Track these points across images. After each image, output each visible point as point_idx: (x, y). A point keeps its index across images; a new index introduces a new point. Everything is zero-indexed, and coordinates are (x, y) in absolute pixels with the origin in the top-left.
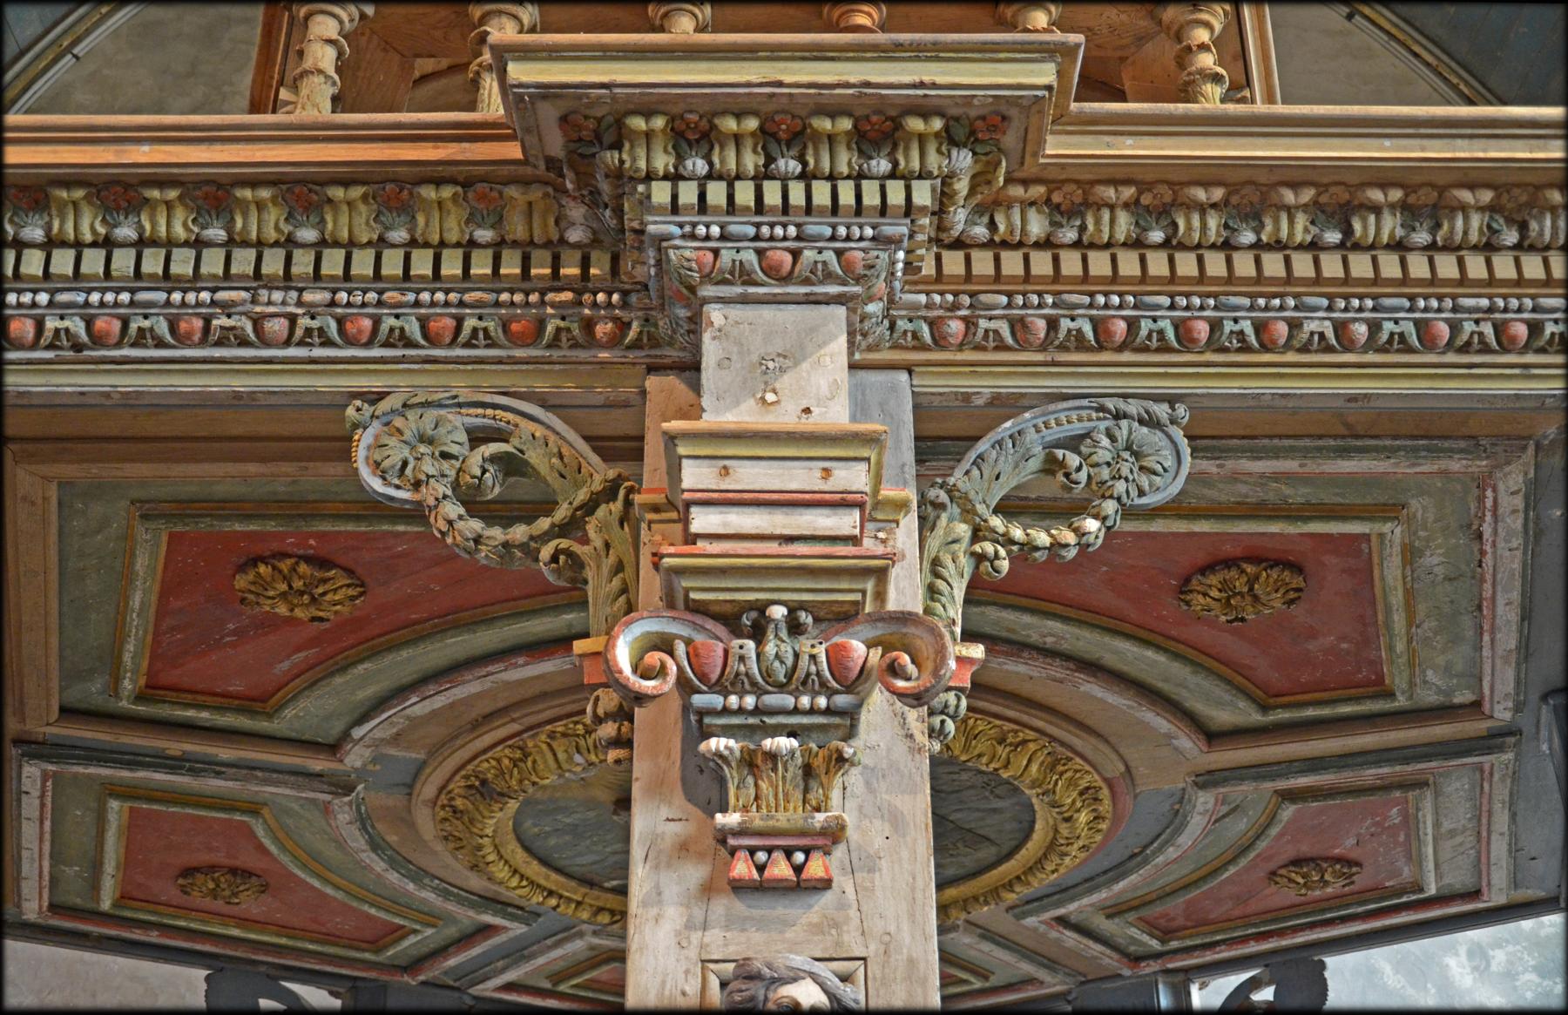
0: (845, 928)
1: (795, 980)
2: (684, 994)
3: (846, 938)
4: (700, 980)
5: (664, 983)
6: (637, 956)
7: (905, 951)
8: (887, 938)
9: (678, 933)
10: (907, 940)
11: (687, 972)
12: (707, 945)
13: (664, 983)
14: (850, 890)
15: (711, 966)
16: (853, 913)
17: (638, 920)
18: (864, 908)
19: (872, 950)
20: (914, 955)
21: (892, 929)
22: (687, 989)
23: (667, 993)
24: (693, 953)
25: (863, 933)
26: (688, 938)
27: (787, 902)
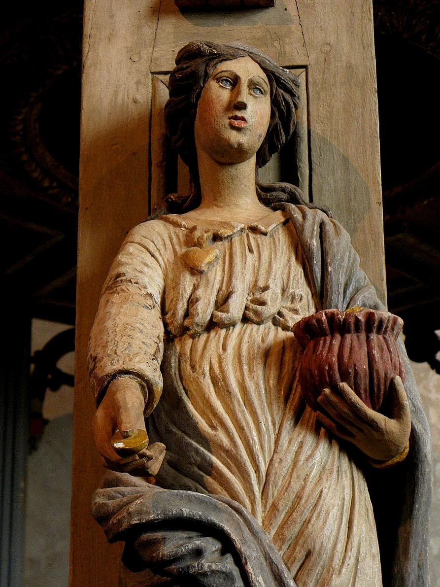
0: (287, 40)
1: (234, 57)
2: (135, 101)
3: (287, 49)
4: (150, 89)
5: (116, 93)
6: (91, 71)
7: (344, 58)
8: (328, 48)
9: (129, 50)
10: (346, 49)
11: (138, 83)
12: (157, 59)
13: (116, 93)
14: (292, 8)
15: (161, 77)
16: (294, 27)
17: (92, 40)
18: (305, 22)
19: (312, 59)
20: (353, 62)
21: (332, 39)
22: (139, 97)
23: (119, 101)
24: (144, 66)
25: (304, 45)
26: (139, 53)
27: (232, 20)
